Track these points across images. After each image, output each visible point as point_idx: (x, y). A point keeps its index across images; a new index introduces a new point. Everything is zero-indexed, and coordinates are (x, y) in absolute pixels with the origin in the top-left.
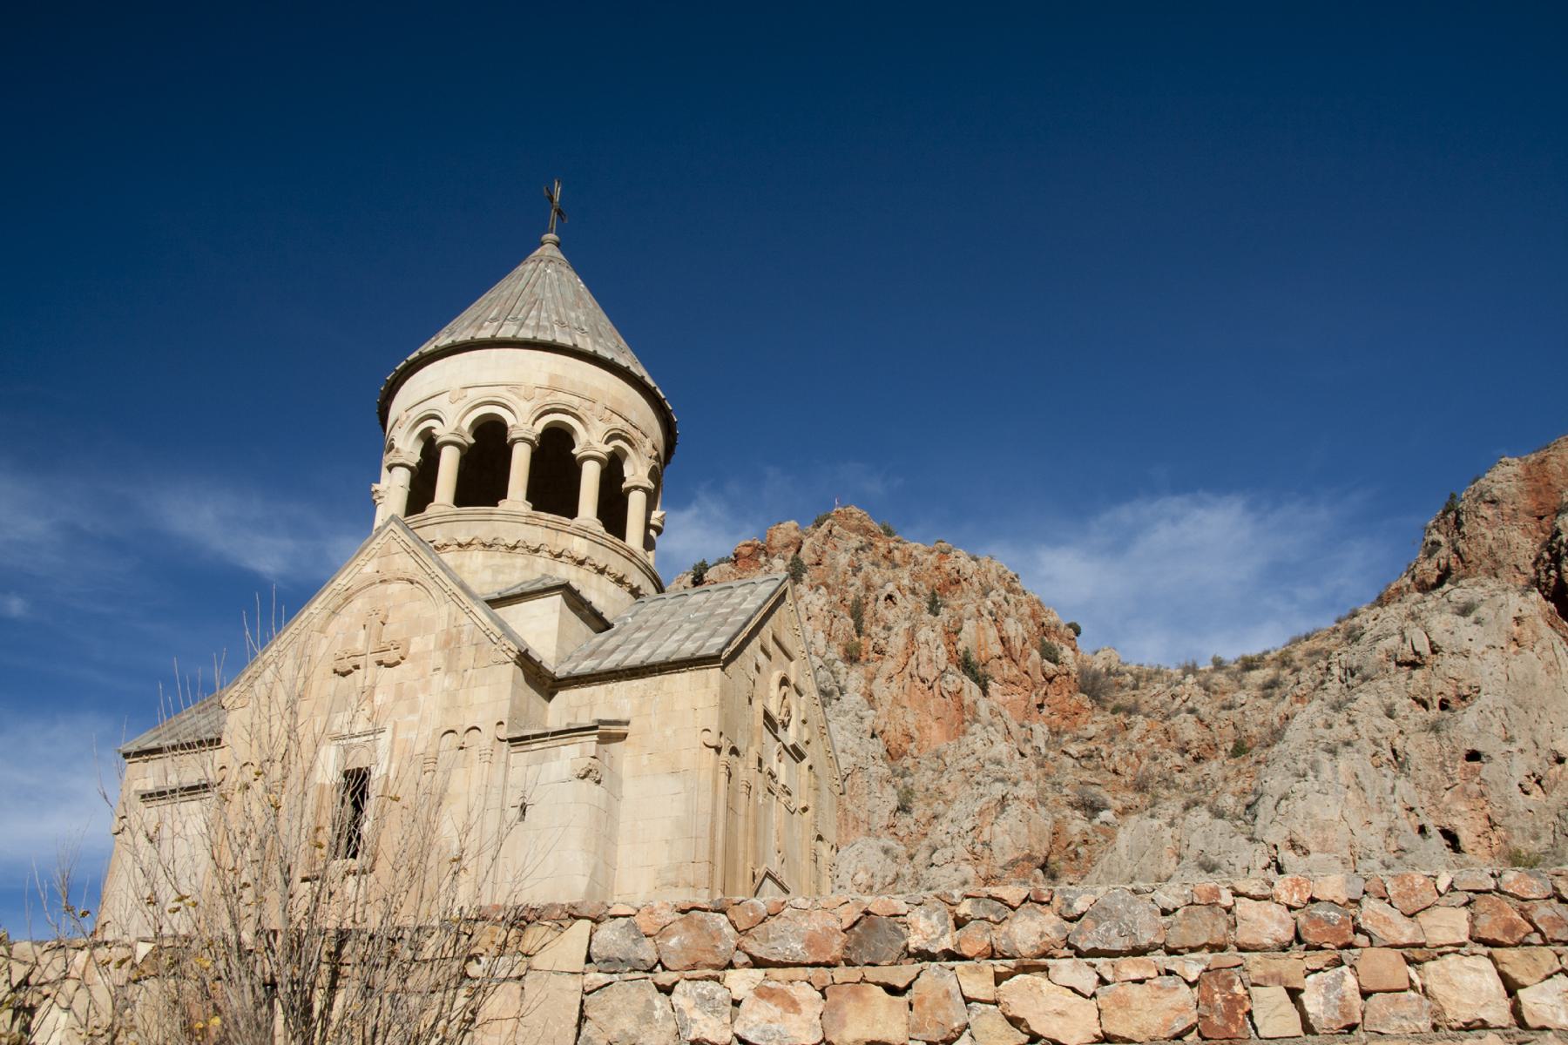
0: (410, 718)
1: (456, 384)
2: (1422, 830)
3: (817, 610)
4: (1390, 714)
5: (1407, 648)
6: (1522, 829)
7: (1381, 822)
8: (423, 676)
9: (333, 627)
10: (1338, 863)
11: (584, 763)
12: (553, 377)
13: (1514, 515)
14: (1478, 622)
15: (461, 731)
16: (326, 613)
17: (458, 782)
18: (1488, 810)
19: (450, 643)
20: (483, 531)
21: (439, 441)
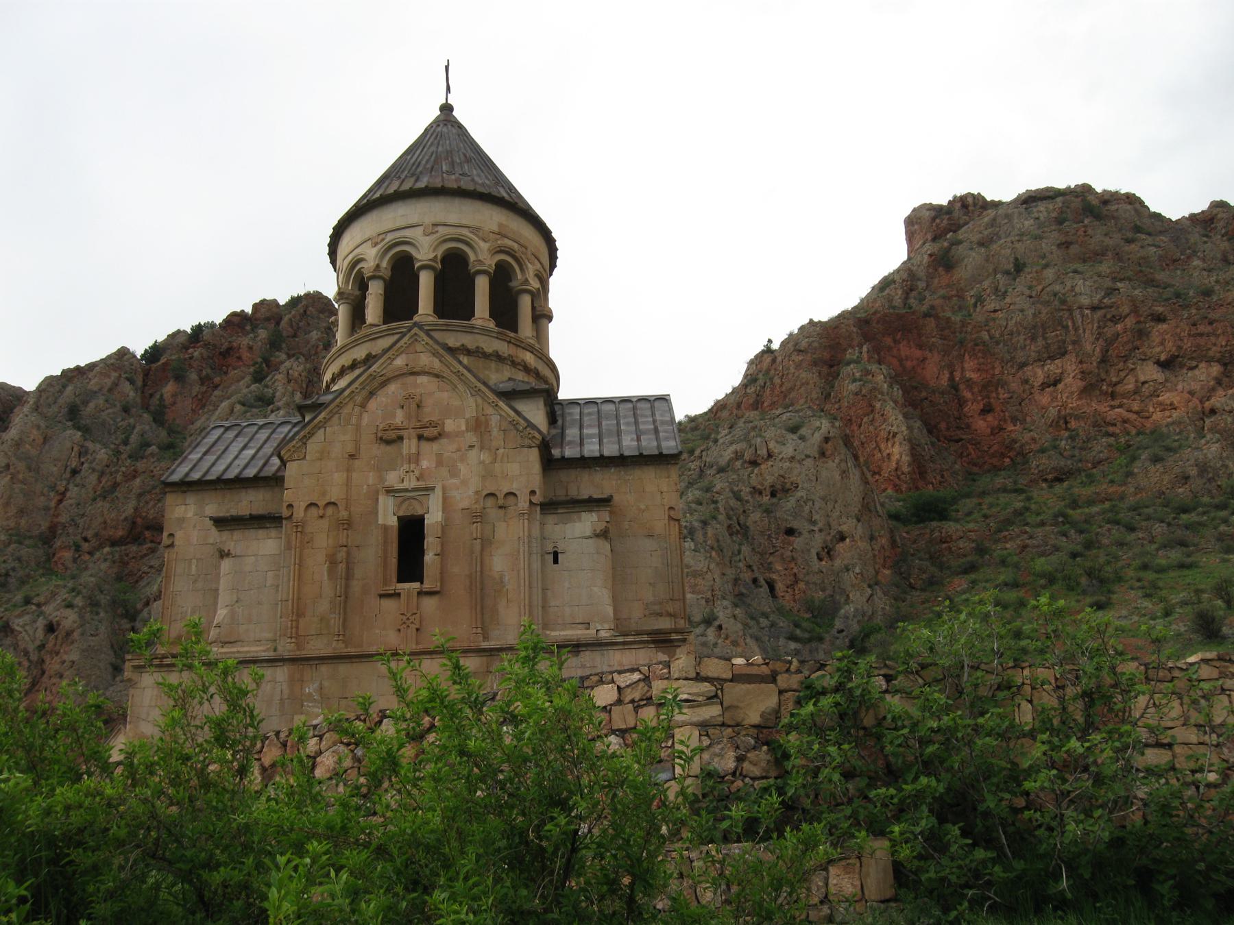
0: (453, 481)
1: (428, 220)
2: (755, 581)
3: (296, 374)
4: (739, 499)
5: (752, 450)
6: (815, 584)
7: (731, 573)
8: (459, 450)
9: (372, 405)
10: (703, 602)
11: (602, 526)
12: (500, 225)
13: (815, 363)
14: (802, 438)
15: (501, 496)
16: (364, 393)
17: (501, 531)
18: (795, 570)
19: (479, 426)
20: (468, 340)
21: (417, 265)
